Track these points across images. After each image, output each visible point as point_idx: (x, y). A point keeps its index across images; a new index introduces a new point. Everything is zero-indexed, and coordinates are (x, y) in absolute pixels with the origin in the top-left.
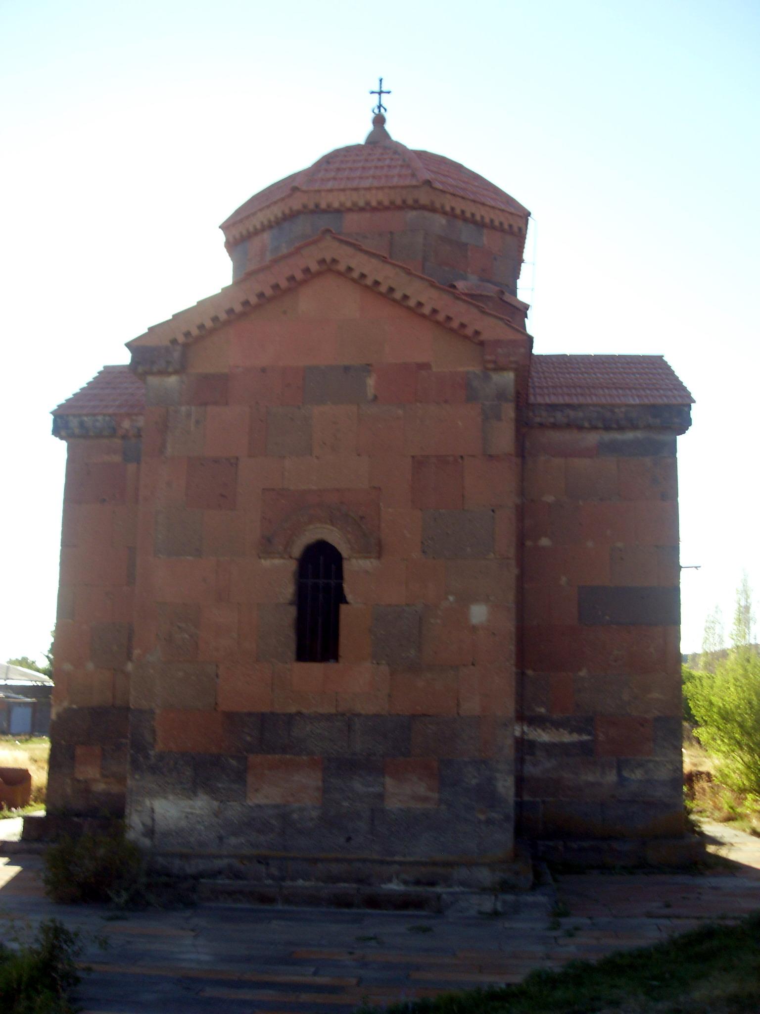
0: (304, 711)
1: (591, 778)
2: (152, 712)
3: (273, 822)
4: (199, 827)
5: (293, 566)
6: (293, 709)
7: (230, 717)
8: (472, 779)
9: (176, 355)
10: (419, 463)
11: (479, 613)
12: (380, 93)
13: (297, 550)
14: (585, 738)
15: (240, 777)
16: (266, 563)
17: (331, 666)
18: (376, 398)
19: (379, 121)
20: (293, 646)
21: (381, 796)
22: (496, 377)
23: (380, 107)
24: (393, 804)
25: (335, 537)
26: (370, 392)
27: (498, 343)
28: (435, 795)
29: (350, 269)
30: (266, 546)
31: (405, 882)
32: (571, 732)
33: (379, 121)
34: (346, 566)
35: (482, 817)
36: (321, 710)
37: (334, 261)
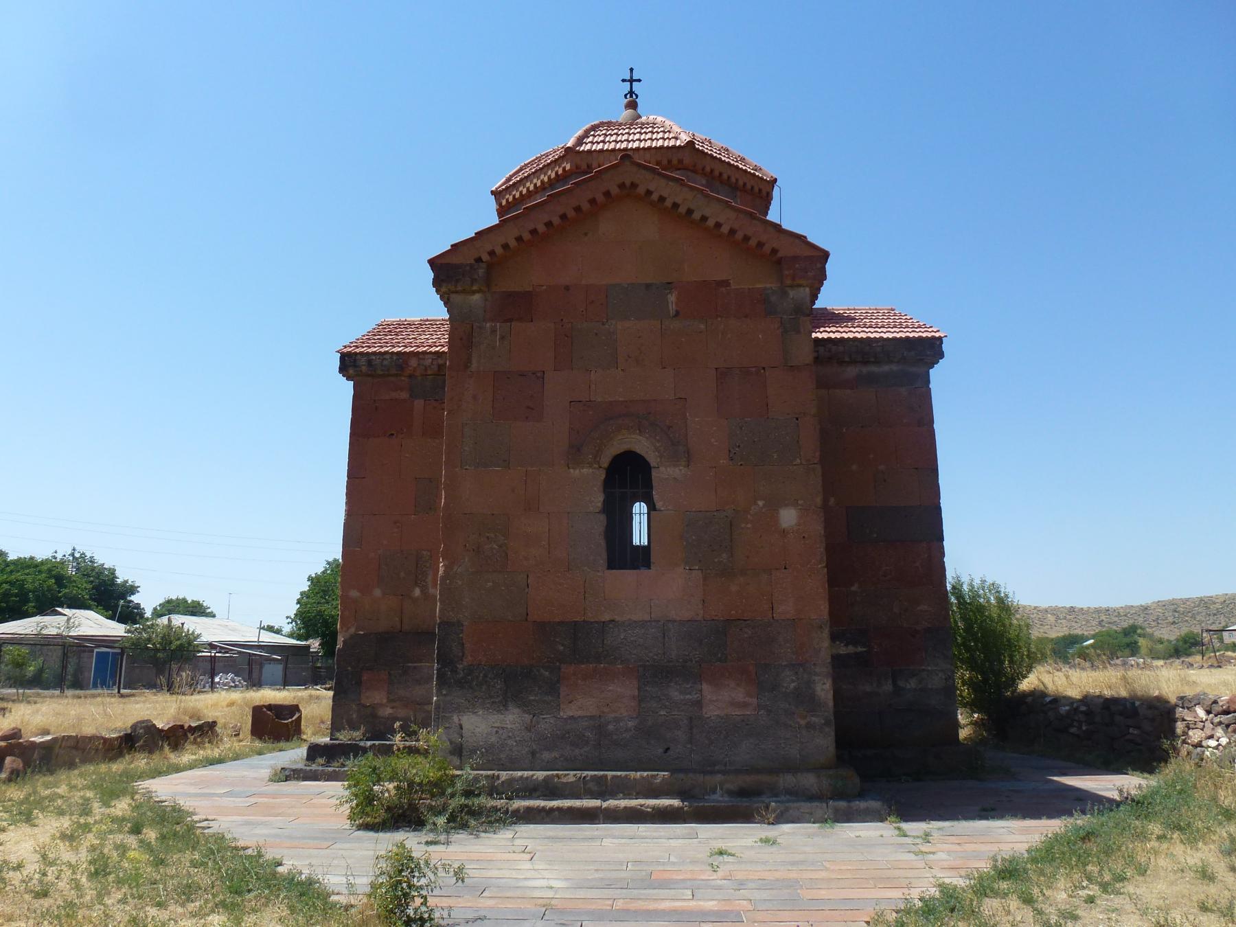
0: (617, 618)
1: (868, 688)
2: (459, 624)
3: (588, 734)
4: (510, 742)
5: (602, 475)
6: (606, 617)
8: (789, 682)
9: (481, 272)
10: (723, 374)
11: (788, 517)
12: (631, 81)
13: (605, 461)
14: (860, 649)
16: (575, 473)
17: (644, 571)
18: (677, 314)
20: (605, 555)
21: (699, 704)
22: (792, 293)
23: (631, 92)
24: (712, 711)
25: (642, 445)
26: (672, 308)
27: (795, 258)
28: (755, 700)
29: (649, 193)
30: (575, 454)
31: (730, 793)
32: (846, 645)
33: (632, 105)
34: (654, 474)
35: (803, 722)
36: (634, 618)
37: (634, 185)
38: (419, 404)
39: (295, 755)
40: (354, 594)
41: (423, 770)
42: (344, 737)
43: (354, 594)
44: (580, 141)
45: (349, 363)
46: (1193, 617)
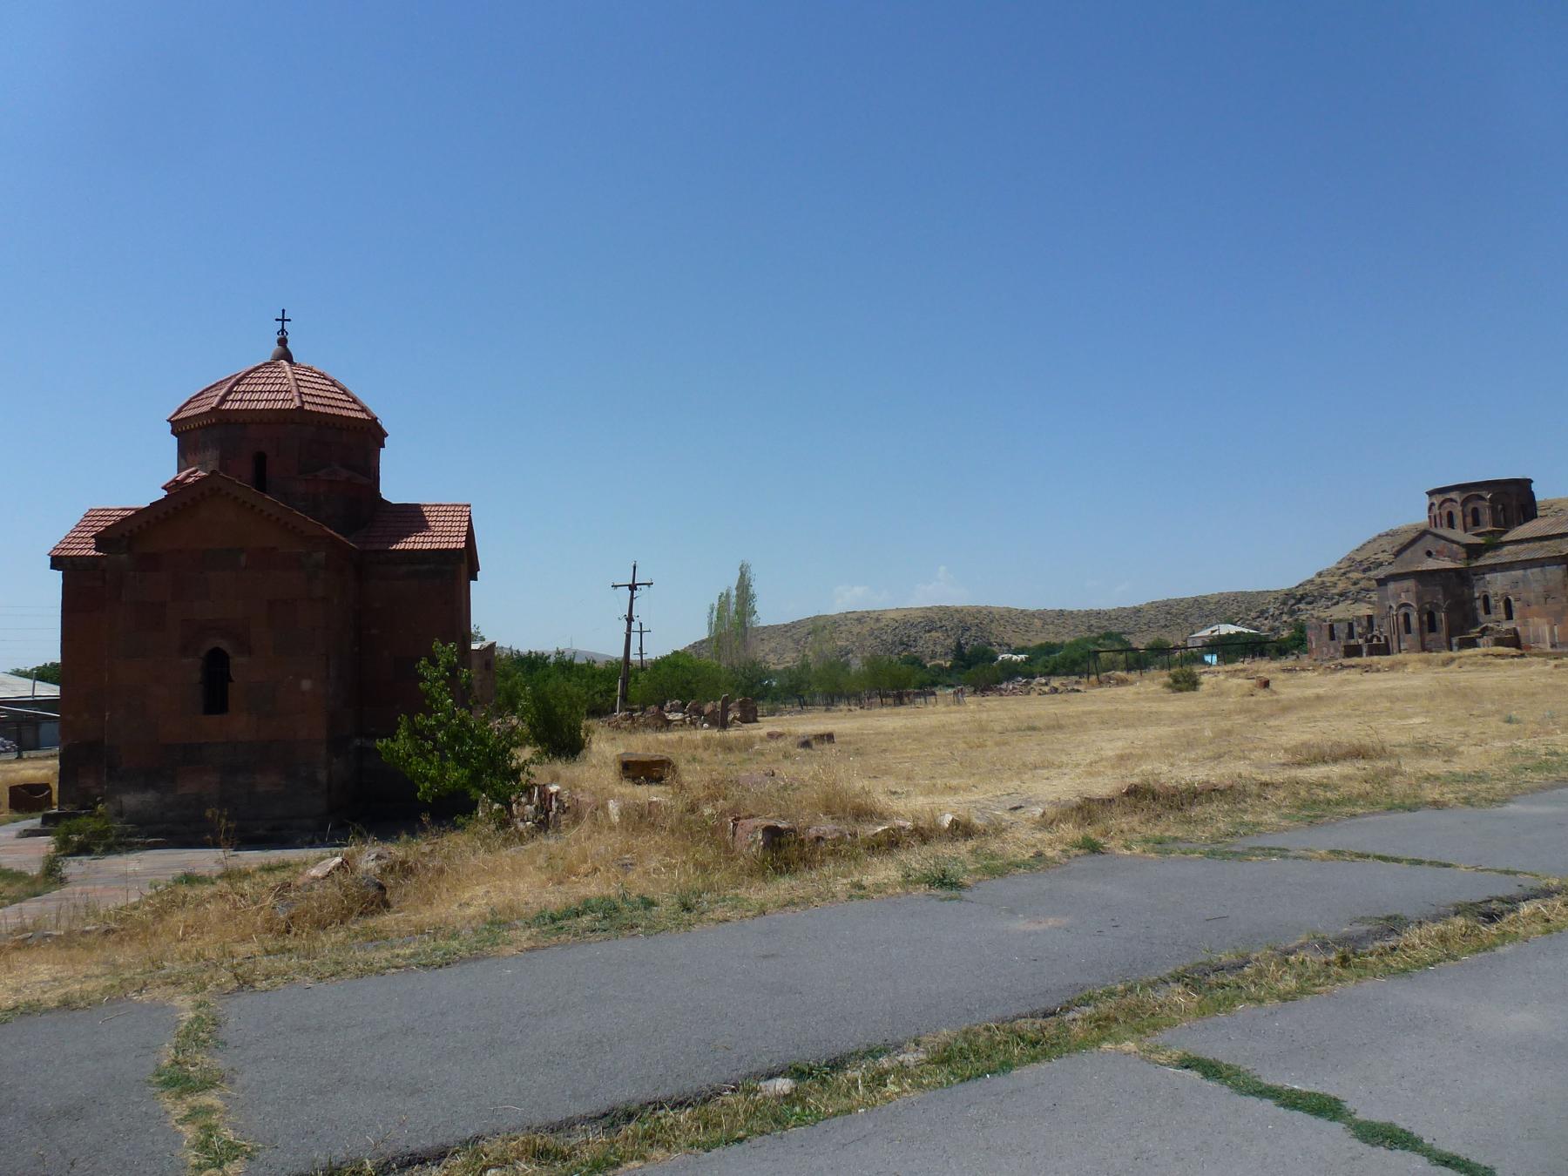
11: (306, 685)
12: (283, 320)
13: (202, 654)
19: (283, 342)
25: (224, 645)
33: (283, 342)
39: (35, 822)
41: (95, 825)
42: (67, 810)
44: (223, 400)
45: (57, 562)
46: (1186, 620)
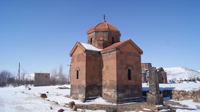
7: (124, 85)
15: (125, 91)
16: (126, 71)
24: (135, 93)
25: (130, 68)
30: (126, 69)
33: (105, 20)
38: (93, 57)
40: (87, 80)
43: (87, 80)
